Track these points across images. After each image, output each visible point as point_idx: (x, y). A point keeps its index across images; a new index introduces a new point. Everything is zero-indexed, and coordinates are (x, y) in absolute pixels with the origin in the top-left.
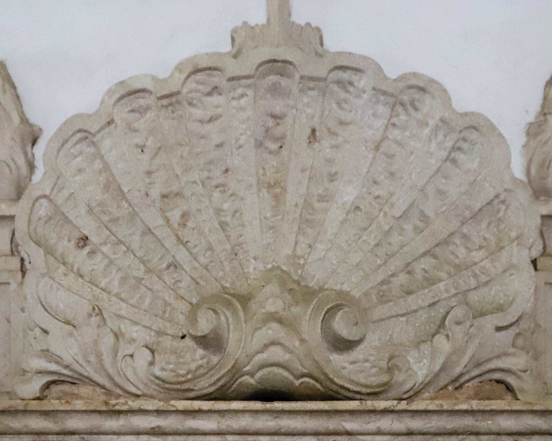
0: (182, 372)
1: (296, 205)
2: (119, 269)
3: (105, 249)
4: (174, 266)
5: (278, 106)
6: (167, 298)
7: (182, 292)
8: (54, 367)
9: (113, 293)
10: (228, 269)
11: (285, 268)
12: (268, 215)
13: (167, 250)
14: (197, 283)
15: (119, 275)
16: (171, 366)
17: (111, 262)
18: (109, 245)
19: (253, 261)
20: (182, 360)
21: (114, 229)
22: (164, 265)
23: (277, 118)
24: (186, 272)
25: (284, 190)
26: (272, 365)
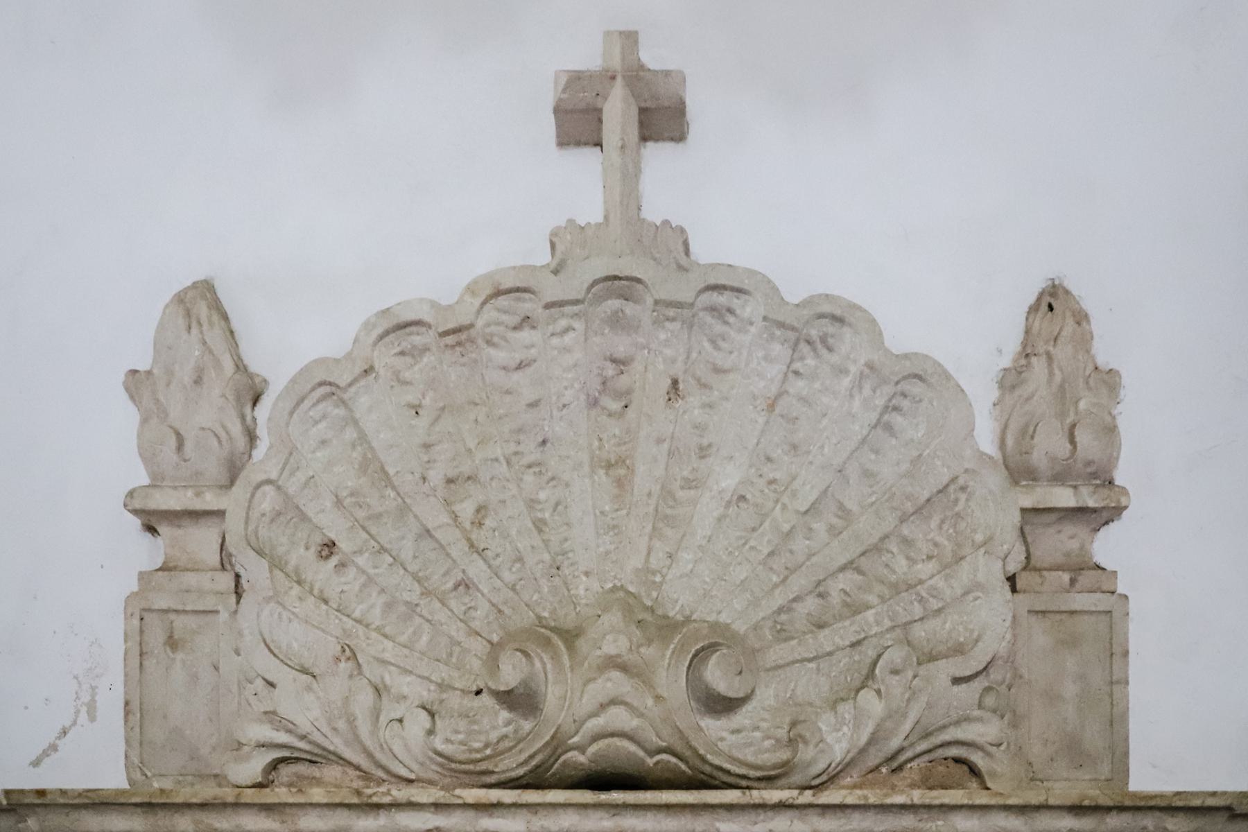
1: (649, 494)
5: (622, 345)
11: (632, 589)
12: (607, 508)
23: (621, 363)
25: (631, 470)
26: (612, 735)
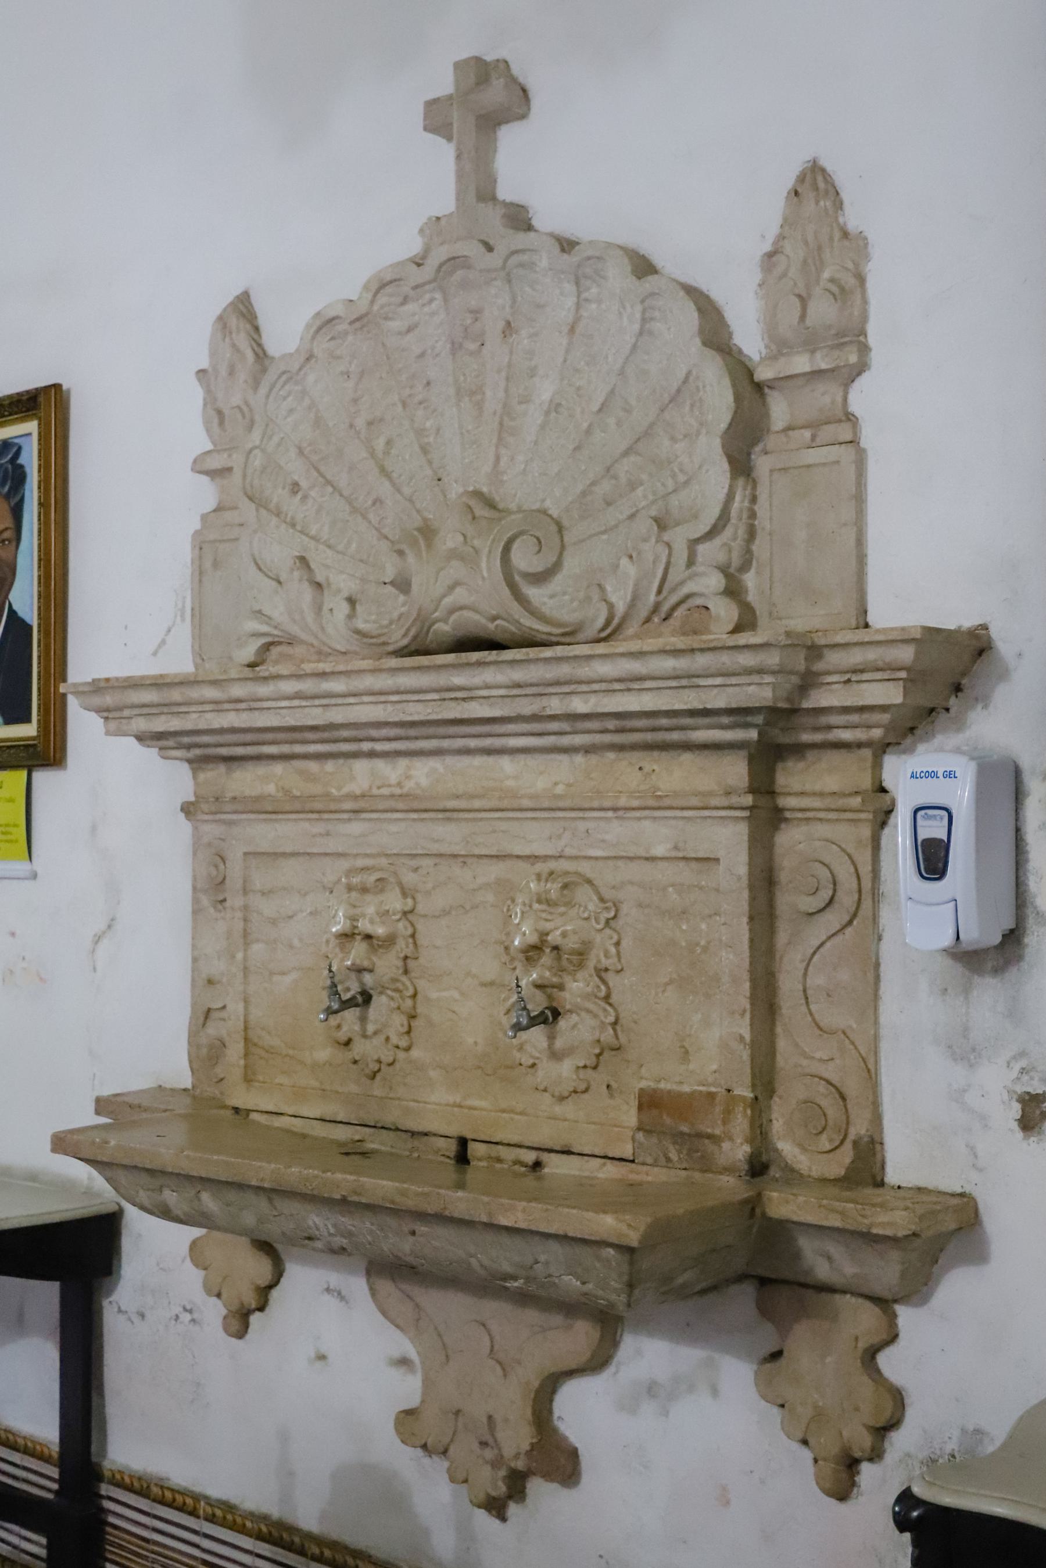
1: (495, 413)
3: (313, 493)
4: (377, 501)
7: (385, 531)
8: (265, 628)
9: (322, 541)
16: (373, 617)
20: (383, 609)
21: (323, 469)
22: (370, 502)
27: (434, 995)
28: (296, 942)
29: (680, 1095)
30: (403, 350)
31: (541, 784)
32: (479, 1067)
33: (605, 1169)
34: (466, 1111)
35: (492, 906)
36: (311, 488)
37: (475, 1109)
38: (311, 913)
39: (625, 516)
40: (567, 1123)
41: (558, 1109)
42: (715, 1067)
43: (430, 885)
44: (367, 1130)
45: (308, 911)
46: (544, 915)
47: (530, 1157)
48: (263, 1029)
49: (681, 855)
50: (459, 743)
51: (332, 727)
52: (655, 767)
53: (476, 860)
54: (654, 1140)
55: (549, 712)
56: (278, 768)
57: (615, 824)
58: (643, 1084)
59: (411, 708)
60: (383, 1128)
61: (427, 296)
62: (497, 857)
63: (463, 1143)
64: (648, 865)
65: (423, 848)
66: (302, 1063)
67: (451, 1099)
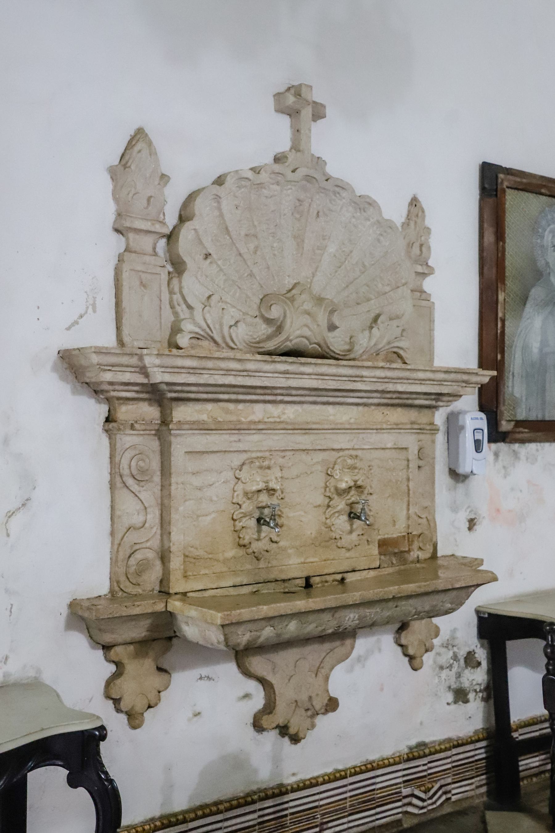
0: (255, 337)
2: (225, 275)
6: (249, 294)
10: (277, 280)
13: (248, 266)
14: (262, 287)
15: (224, 278)
16: (251, 333)
17: (221, 270)
18: (221, 261)
19: (287, 278)
24: (257, 280)
27: (291, 515)
28: (215, 498)
29: (394, 538)
30: (266, 205)
31: (345, 418)
32: (313, 544)
33: (369, 574)
34: (310, 564)
35: (321, 472)
36: (219, 259)
37: (312, 562)
38: (224, 482)
39: (366, 310)
40: (354, 559)
41: (348, 555)
42: (404, 526)
43: (290, 464)
44: (260, 585)
45: (222, 481)
46: (351, 474)
47: (339, 577)
48: (192, 547)
49: (396, 447)
50: (325, 399)
51: (290, 388)
52: (388, 413)
53: (313, 451)
54: (388, 557)
55: (389, 390)
56: (210, 406)
57: (374, 434)
58: (379, 537)
59: (330, 382)
60: (268, 582)
61: (289, 187)
62: (324, 450)
63: (308, 579)
64: (382, 451)
65: (291, 447)
66: (218, 561)
67: (300, 562)
